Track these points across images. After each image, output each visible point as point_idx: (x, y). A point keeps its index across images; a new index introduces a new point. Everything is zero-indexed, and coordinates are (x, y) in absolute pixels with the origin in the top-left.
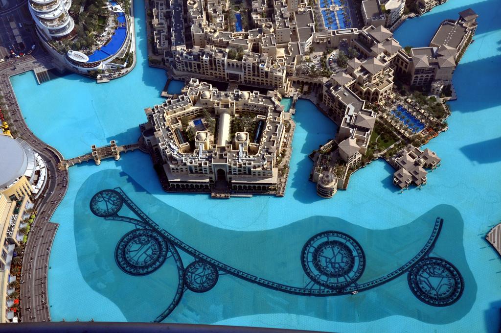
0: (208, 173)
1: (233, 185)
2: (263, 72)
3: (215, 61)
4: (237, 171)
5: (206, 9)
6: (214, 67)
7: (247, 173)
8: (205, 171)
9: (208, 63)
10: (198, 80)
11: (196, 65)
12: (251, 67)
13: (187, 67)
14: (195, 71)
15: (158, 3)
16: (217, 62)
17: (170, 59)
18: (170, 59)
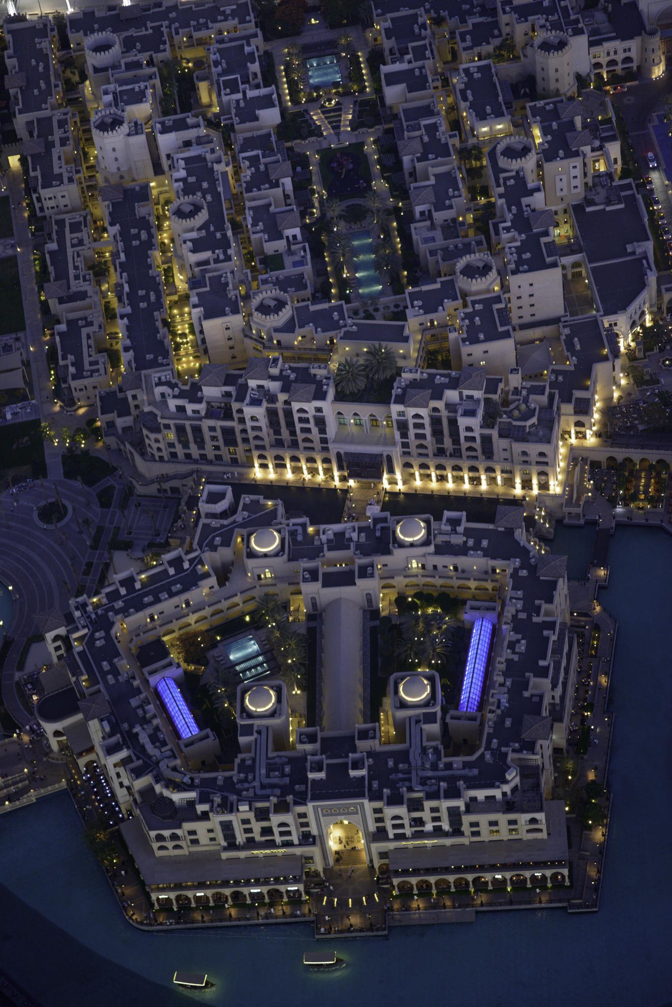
0: (296, 842)
1: (396, 881)
2: (473, 439)
3: (289, 414)
4: (406, 822)
5: (237, 227)
6: (285, 434)
7: (446, 827)
8: (282, 834)
9: (263, 422)
10: (229, 490)
11: (219, 433)
12: (427, 421)
13: (186, 445)
14: (219, 458)
15: (61, 223)
16: (296, 416)
17: (121, 422)
18: (121, 422)
